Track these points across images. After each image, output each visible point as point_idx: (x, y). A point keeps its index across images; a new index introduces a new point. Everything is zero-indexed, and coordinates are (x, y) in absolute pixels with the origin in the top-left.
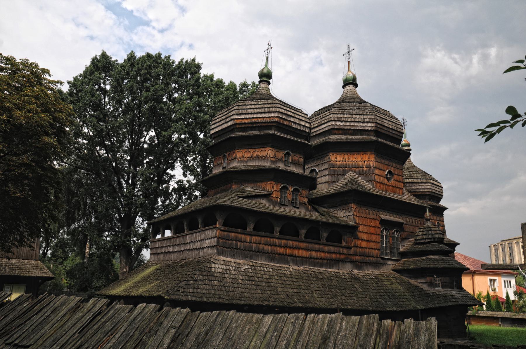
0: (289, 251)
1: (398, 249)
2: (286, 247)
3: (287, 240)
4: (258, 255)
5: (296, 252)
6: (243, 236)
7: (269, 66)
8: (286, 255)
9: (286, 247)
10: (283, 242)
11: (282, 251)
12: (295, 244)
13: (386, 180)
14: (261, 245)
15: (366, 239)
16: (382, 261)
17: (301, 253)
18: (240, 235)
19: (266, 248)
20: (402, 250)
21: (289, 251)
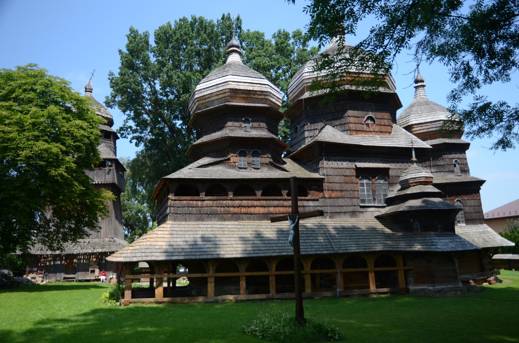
0: (243, 210)
1: (386, 195)
2: (240, 206)
3: (241, 200)
4: (211, 217)
5: (252, 210)
6: (195, 202)
7: (91, 84)
8: (241, 214)
9: (240, 206)
10: (237, 203)
11: (236, 210)
12: (250, 203)
13: (365, 126)
14: (213, 208)
15: (338, 189)
16: (362, 210)
17: (257, 210)
18: (191, 202)
19: (219, 209)
20: (391, 195)
21: (243, 210)
